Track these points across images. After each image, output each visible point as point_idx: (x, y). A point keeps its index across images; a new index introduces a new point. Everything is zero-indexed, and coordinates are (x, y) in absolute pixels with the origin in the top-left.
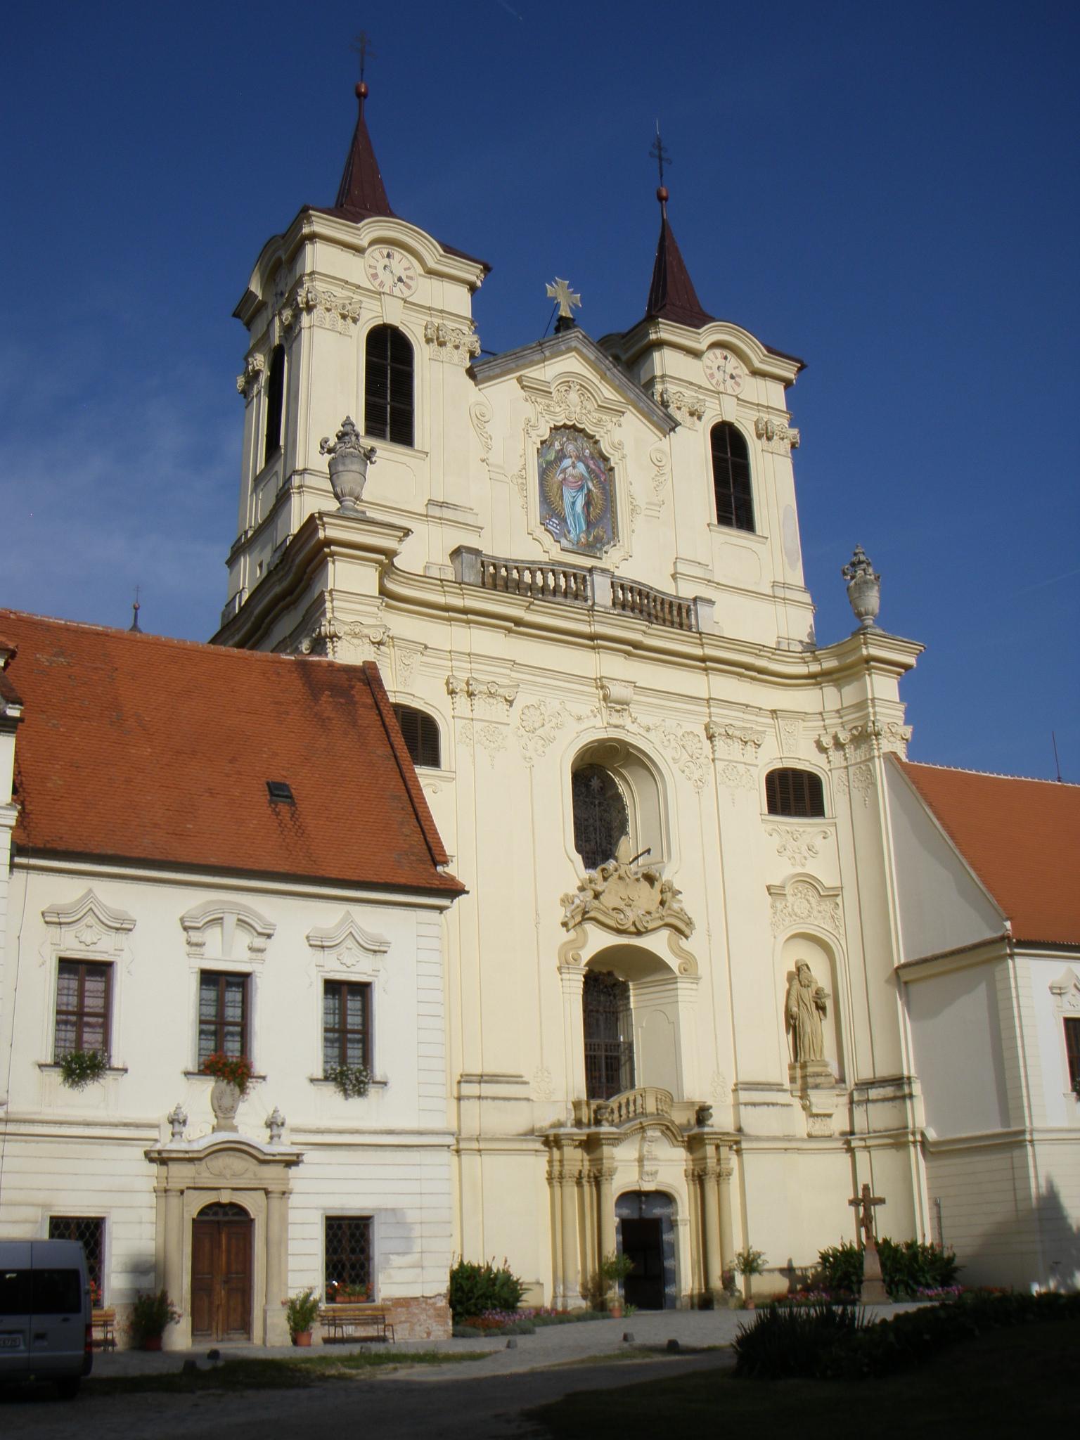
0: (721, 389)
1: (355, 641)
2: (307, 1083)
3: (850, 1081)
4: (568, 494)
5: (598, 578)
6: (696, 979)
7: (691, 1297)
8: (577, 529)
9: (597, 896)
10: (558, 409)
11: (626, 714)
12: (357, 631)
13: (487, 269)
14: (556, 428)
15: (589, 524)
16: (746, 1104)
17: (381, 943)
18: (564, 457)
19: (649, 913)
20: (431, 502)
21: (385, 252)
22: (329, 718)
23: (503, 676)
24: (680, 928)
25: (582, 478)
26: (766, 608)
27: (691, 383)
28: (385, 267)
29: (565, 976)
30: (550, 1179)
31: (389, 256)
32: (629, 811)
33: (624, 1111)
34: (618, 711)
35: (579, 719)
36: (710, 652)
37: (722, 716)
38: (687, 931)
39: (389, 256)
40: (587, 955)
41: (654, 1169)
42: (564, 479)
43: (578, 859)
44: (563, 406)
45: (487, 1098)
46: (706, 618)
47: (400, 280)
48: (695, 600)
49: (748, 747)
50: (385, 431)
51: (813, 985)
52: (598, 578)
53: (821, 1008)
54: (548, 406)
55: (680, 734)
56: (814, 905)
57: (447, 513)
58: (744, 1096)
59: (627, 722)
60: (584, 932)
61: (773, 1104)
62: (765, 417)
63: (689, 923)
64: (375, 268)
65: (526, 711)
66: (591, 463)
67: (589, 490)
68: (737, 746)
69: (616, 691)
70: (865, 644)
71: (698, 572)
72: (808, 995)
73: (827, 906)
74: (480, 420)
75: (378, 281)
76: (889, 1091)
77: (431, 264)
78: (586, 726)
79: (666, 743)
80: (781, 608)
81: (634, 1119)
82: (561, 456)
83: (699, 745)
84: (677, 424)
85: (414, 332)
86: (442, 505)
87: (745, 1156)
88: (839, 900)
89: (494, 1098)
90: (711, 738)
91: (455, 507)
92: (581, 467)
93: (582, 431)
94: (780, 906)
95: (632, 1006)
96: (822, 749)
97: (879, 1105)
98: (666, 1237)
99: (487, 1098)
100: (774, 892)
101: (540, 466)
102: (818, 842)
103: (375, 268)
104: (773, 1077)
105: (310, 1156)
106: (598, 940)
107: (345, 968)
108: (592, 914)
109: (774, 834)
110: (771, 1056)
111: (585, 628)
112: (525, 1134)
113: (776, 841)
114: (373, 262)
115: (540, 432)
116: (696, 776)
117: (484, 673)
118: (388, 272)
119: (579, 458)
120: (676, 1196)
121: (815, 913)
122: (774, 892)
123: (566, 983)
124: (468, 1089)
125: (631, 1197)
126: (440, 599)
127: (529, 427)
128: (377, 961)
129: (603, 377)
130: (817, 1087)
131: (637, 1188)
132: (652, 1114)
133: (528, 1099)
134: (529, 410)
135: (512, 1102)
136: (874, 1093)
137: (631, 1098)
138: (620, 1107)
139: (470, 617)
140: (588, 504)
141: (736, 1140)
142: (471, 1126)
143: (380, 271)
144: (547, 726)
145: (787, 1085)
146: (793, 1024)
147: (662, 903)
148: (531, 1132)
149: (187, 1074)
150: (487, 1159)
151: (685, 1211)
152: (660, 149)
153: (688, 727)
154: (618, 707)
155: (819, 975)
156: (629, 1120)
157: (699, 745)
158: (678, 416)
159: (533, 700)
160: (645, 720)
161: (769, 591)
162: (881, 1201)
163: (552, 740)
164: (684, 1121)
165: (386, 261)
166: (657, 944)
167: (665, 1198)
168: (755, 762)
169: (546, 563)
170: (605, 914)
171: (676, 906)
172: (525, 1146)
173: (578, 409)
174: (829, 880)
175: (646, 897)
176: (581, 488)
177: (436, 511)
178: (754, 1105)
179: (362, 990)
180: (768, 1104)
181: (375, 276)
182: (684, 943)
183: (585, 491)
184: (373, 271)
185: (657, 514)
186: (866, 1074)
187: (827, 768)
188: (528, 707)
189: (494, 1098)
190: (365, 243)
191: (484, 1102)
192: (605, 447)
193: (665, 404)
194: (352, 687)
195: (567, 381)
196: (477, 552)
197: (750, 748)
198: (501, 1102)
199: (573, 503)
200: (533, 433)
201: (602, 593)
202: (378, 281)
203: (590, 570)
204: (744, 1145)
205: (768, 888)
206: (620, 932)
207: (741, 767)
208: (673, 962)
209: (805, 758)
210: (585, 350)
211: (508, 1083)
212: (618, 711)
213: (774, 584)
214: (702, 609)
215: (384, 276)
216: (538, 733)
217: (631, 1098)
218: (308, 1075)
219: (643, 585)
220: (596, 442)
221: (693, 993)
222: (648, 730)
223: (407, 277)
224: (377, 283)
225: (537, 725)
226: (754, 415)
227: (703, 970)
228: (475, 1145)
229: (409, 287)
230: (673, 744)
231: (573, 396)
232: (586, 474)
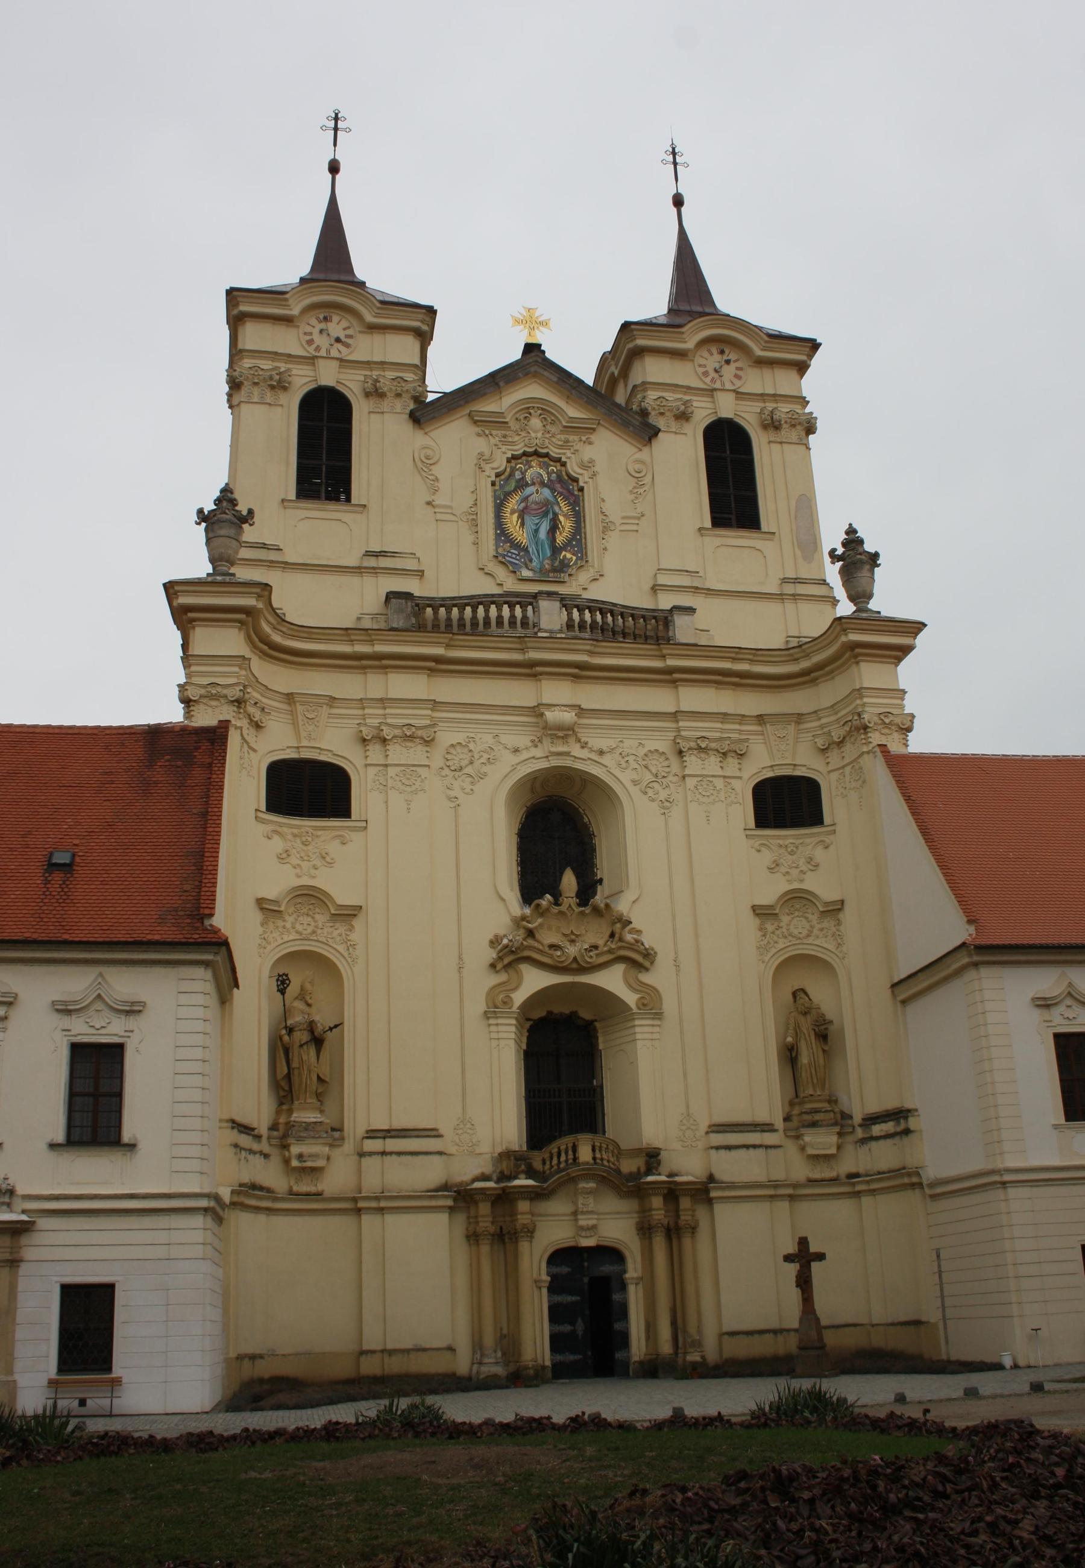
0: (718, 385)
1: (214, 703)
2: (45, 1147)
3: (857, 1119)
4: (530, 521)
5: (544, 604)
6: (659, 1015)
7: (641, 1363)
8: (540, 558)
9: (530, 933)
10: (517, 438)
11: (572, 740)
12: (214, 692)
14: (514, 457)
15: (555, 550)
16: (717, 1148)
17: (133, 1003)
18: (527, 485)
19: (596, 947)
20: (369, 554)
21: (321, 317)
22: (156, 783)
23: (420, 718)
24: (638, 959)
25: (546, 503)
26: (773, 608)
27: (676, 386)
28: (321, 331)
29: (492, 1021)
30: (468, 1237)
31: (325, 319)
32: (596, 841)
33: (555, 1161)
34: (563, 738)
35: (516, 751)
36: (671, 662)
37: (691, 729)
38: (647, 964)
39: (325, 319)
40: (519, 997)
41: (591, 1223)
42: (526, 508)
44: (523, 434)
45: (391, 1153)
46: (683, 629)
47: (338, 340)
48: (671, 610)
49: (730, 760)
50: (319, 491)
51: (814, 1012)
52: (544, 604)
53: (823, 1037)
54: (505, 436)
55: (642, 751)
56: (815, 922)
57: (384, 562)
58: (718, 1139)
59: (576, 750)
60: (519, 974)
61: (754, 1146)
62: (770, 406)
63: (649, 955)
64: (311, 334)
65: (452, 750)
66: (558, 486)
67: (555, 515)
68: (713, 760)
69: (550, 716)
70: (845, 630)
71: (685, 581)
72: (806, 1024)
74: (425, 465)
75: (314, 346)
76: (889, 1127)
77: (369, 318)
78: (513, 759)
79: (624, 765)
80: (790, 606)
81: (564, 1170)
82: (522, 484)
83: (666, 763)
84: (654, 432)
85: (351, 385)
86: (377, 555)
87: (718, 1207)
89: (399, 1154)
90: (680, 753)
91: (393, 554)
92: (546, 492)
93: (547, 455)
94: (770, 927)
95: (601, 1047)
97: (882, 1142)
98: (616, 1297)
99: (391, 1153)
100: (762, 913)
101: (495, 497)
102: (819, 854)
103: (311, 334)
104: (762, 1116)
105: (43, 1223)
106: (534, 981)
107: (95, 1032)
108: (526, 953)
109: (763, 849)
110: (759, 1092)
111: (516, 656)
112: (436, 1190)
113: (767, 857)
114: (308, 329)
115: (495, 465)
116: (663, 795)
117: (398, 717)
118: (325, 335)
119: (542, 484)
120: (627, 1253)
121: (816, 932)
122: (762, 913)
123: (493, 1028)
124: (371, 1145)
125: (560, 1256)
126: (346, 648)
127: (482, 460)
128: (132, 1022)
129: (568, 399)
130: (814, 1124)
131: (572, 1244)
132: (587, 1163)
133: (440, 1153)
134: (482, 445)
135: (421, 1157)
136: (877, 1130)
137: (563, 1147)
138: (551, 1158)
139: (385, 662)
140: (554, 528)
141: (704, 1191)
142: (372, 1182)
143: (316, 336)
144: (477, 763)
145: (779, 1124)
146: (790, 1055)
147: (612, 935)
148: (445, 1187)
149: (53, 1146)
150: (389, 1218)
151: (633, 1270)
152: (674, 153)
153: (651, 745)
154: (560, 734)
155: (821, 995)
156: (559, 1171)
157: (666, 763)
158: (661, 423)
159: (460, 737)
160: (596, 743)
161: (774, 590)
162: (821, 1257)
163: (483, 776)
164: (634, 1169)
165: (323, 326)
166: (612, 980)
167: (612, 1254)
168: (738, 774)
169: (500, 595)
170: (540, 952)
171: (629, 937)
172: (434, 1203)
173: (540, 435)
175: (594, 934)
176: (546, 514)
177: (372, 562)
178: (729, 1148)
179: (114, 1053)
180: (747, 1147)
181: (310, 342)
182: (645, 978)
183: (551, 516)
184: (308, 338)
185: (635, 528)
186: (874, 1107)
188: (452, 745)
189: (399, 1154)
190: (295, 311)
191: (387, 1159)
192: (573, 468)
193: (644, 413)
194: (197, 748)
195: (527, 408)
196: (407, 596)
197: (732, 762)
198: (409, 1157)
199: (537, 531)
200: (487, 467)
201: (551, 616)
202: (314, 346)
203: (535, 596)
204: (713, 1194)
205: (754, 908)
207: (719, 783)
208: (630, 998)
209: (803, 761)
210: (546, 373)
211: (417, 1137)
212: (563, 738)
213: (785, 581)
214: (680, 621)
215: (322, 341)
216: (466, 771)
217: (563, 1147)
218: (48, 1140)
219: (603, 602)
220: (564, 464)
221: (657, 1029)
222: (601, 753)
223: (347, 336)
224: (311, 349)
225: (464, 763)
226: (757, 406)
227: (669, 1005)
228: (374, 1204)
229: (347, 346)
230: (634, 765)
231: (536, 422)
232: (551, 499)
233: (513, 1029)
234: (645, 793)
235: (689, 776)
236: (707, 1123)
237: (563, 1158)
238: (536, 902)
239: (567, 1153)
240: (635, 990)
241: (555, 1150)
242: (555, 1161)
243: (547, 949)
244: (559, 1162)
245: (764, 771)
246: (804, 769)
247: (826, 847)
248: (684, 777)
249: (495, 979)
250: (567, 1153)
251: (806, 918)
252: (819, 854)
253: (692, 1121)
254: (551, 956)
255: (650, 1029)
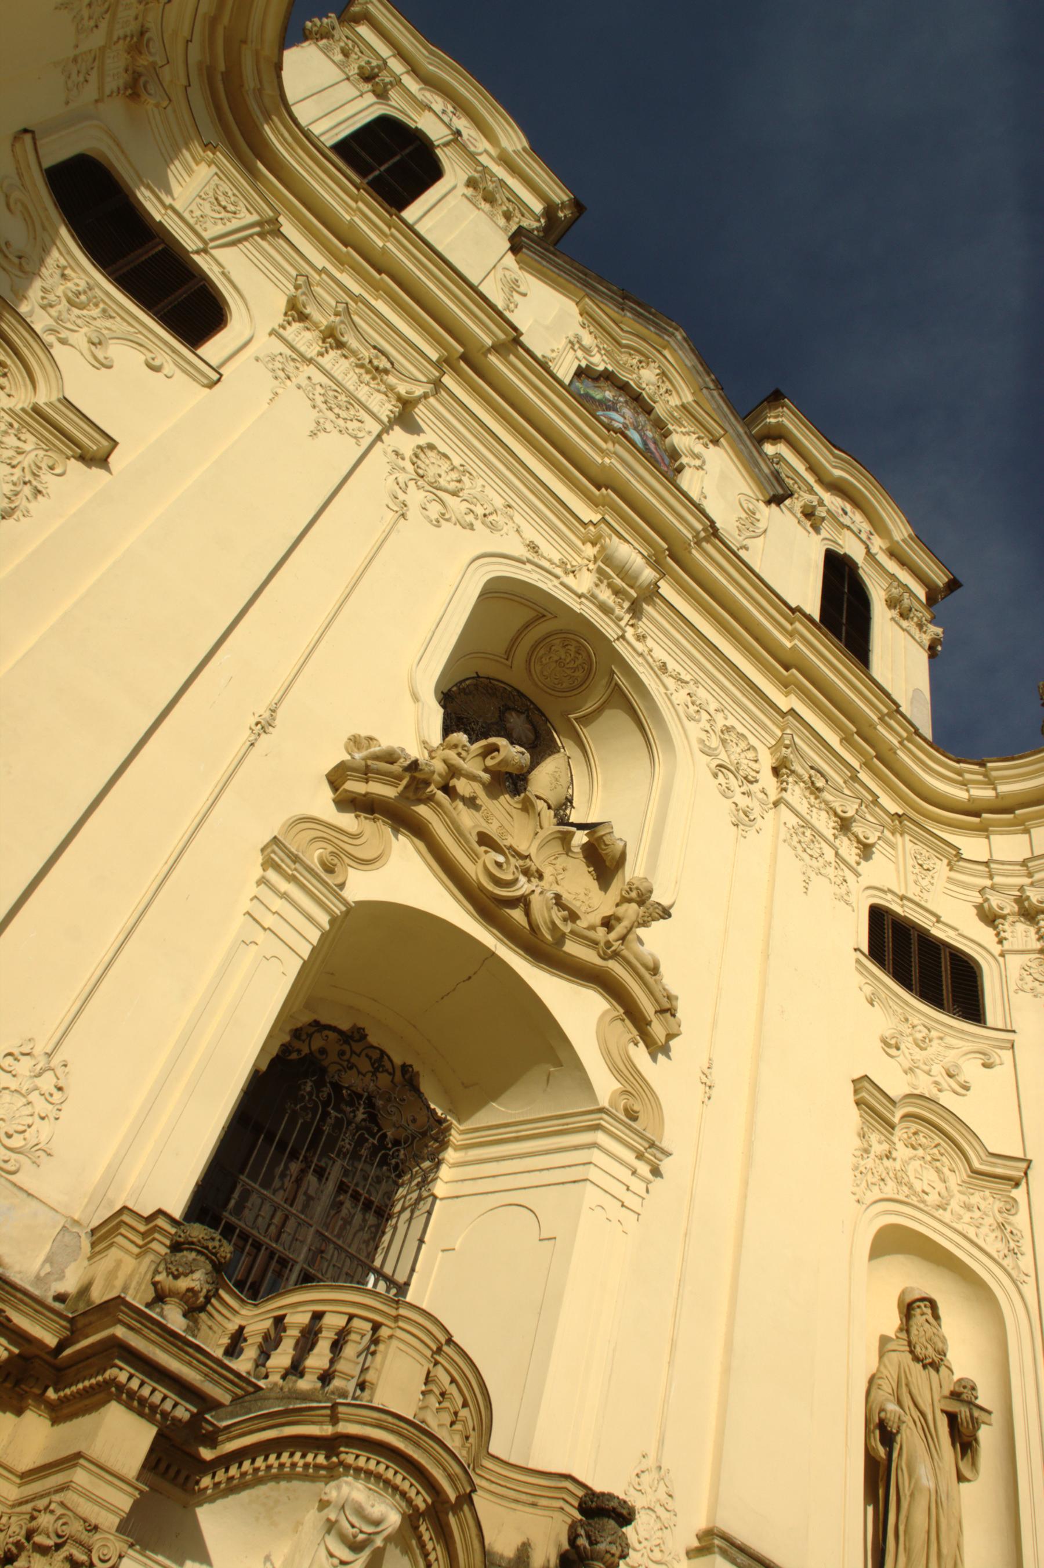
13: (578, 206)
24: (643, 1014)
29: (272, 875)
33: (282, 1358)
40: (362, 887)
43: (436, 715)
53: (964, 1442)
63: (667, 1010)
72: (931, 1392)
73: (986, 1200)
88: (1019, 1193)
95: (439, 1189)
96: (990, 918)
102: (971, 1069)
121: (954, 1205)
137: (333, 1321)
138: (269, 1344)
174: (999, 1137)
187: (996, 949)
206: (488, 907)
217: (333, 1321)
233: (315, 936)
234: (716, 776)
235: (788, 805)
236: (701, 1523)
237: (318, 1359)
238: (492, 740)
239: (337, 1346)
240: (615, 1070)
241: (298, 1319)
242: (282, 1358)
243: (473, 839)
244: (296, 1369)
245: (889, 896)
246: (952, 933)
247: (985, 1065)
248: (776, 804)
249: (322, 803)
250: (337, 1346)
251: (938, 1170)
252: (971, 1069)
253: (661, 1494)
254: (474, 858)
255: (624, 1174)
